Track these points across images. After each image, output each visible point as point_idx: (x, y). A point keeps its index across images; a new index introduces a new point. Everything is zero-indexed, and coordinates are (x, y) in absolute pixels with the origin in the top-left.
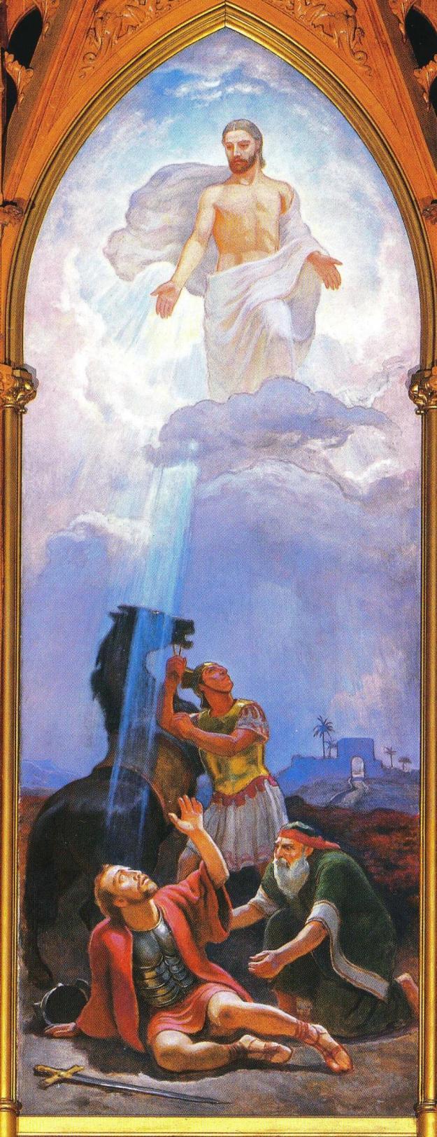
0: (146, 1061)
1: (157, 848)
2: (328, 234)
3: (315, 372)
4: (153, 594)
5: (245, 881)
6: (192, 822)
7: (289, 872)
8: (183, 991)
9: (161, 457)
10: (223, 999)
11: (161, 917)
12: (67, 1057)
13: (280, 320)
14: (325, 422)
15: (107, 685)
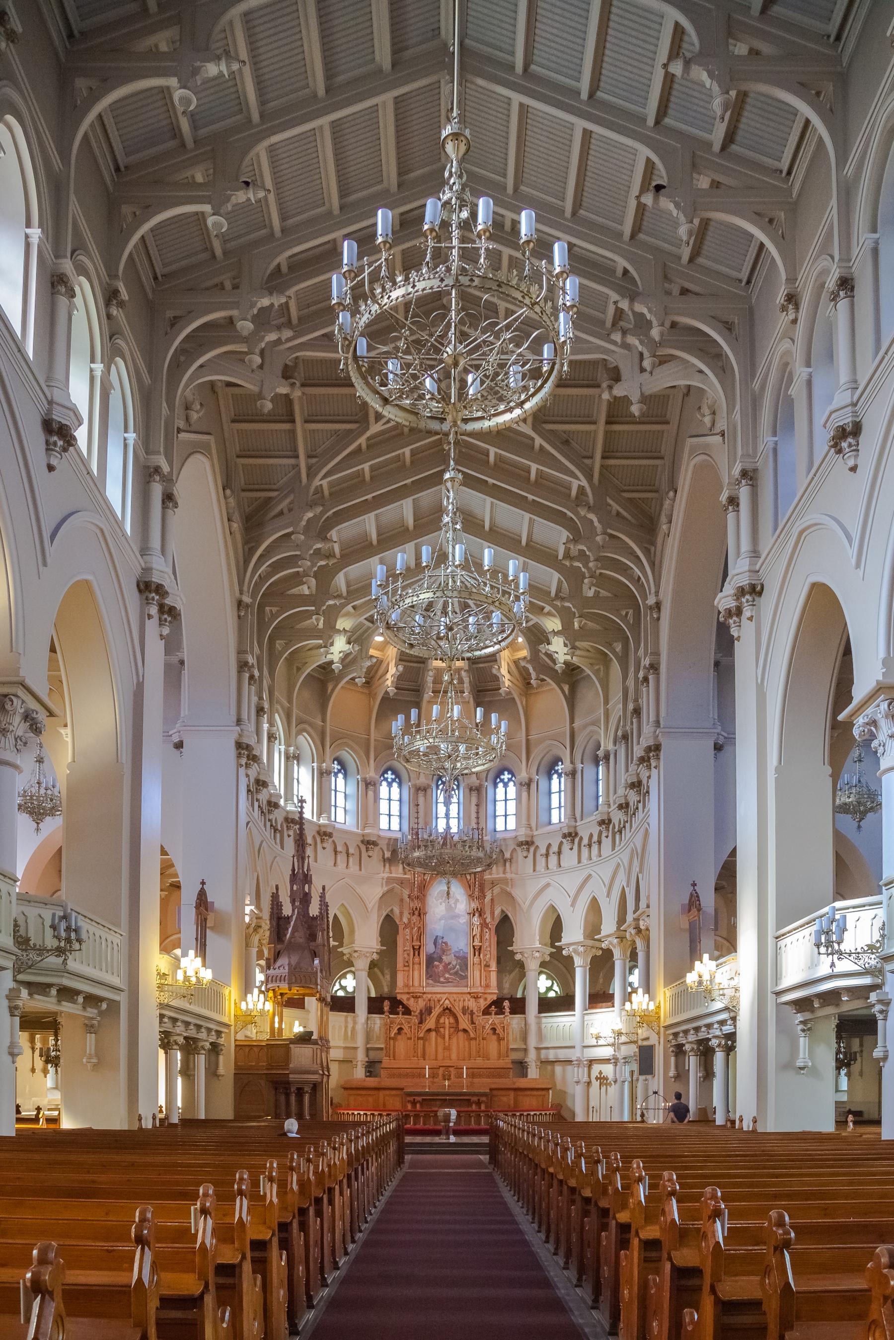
0: (439, 982)
1: (440, 960)
2: (458, 897)
3: (457, 911)
4: (440, 934)
5: (450, 963)
6: (444, 957)
7: (454, 963)
8: (443, 976)
9: (440, 920)
10: (447, 976)
11: (441, 968)
12: (431, 982)
13: (453, 905)
14: (457, 916)
15: (435, 943)
